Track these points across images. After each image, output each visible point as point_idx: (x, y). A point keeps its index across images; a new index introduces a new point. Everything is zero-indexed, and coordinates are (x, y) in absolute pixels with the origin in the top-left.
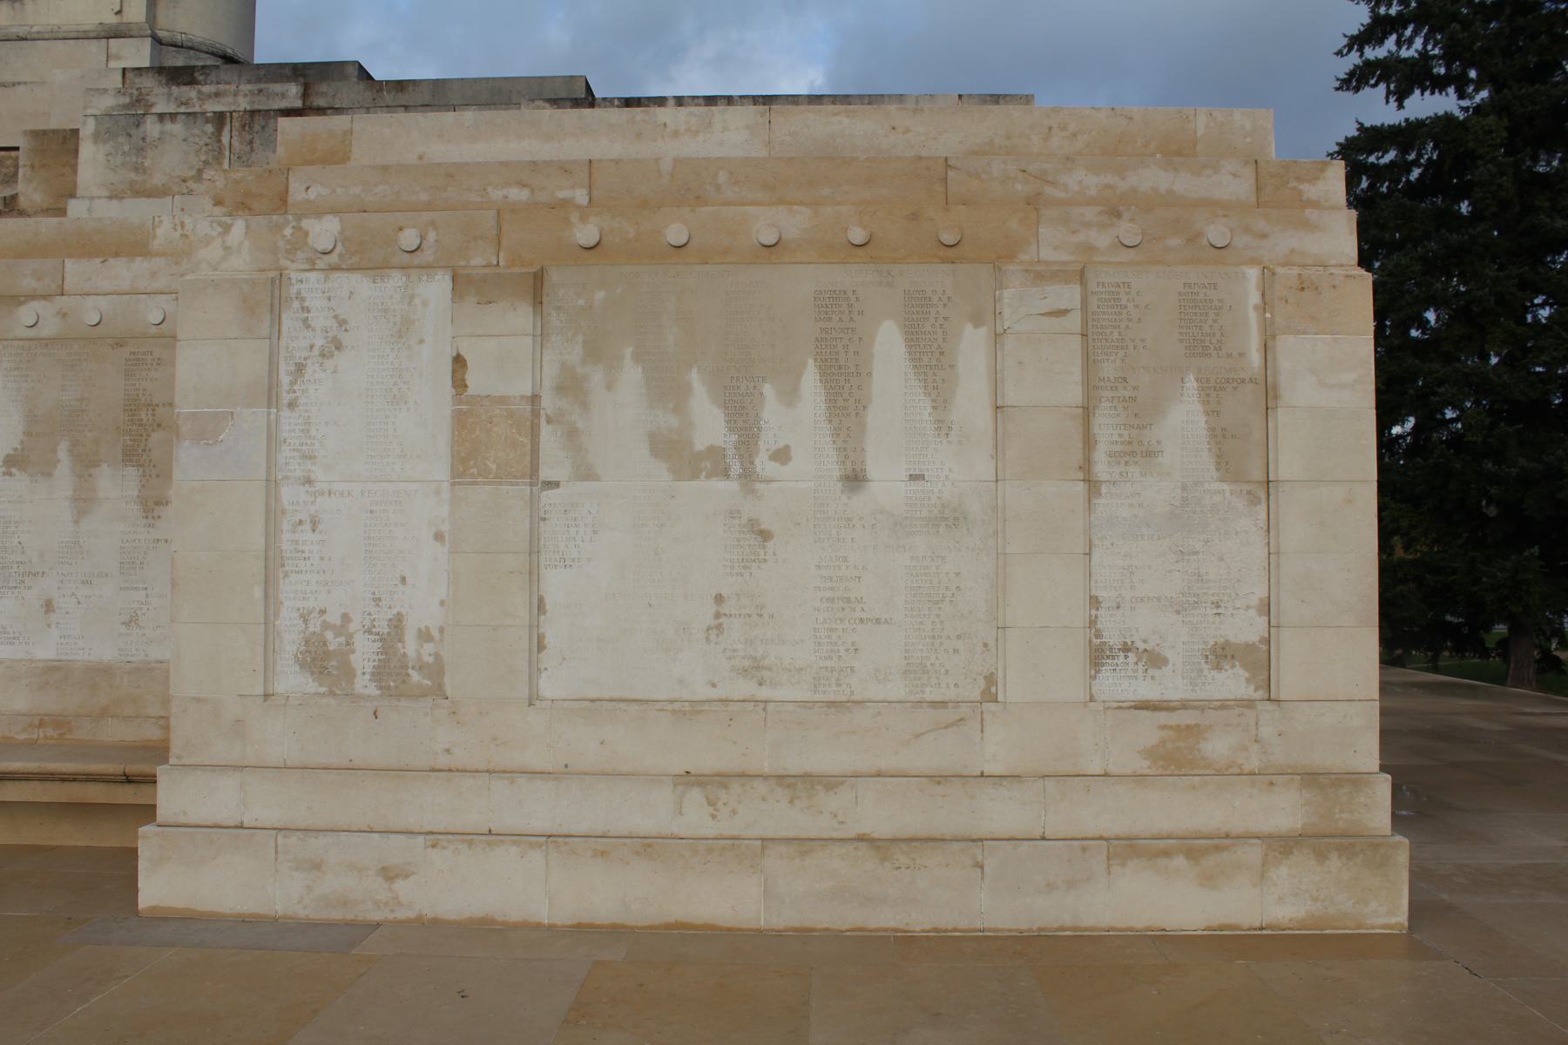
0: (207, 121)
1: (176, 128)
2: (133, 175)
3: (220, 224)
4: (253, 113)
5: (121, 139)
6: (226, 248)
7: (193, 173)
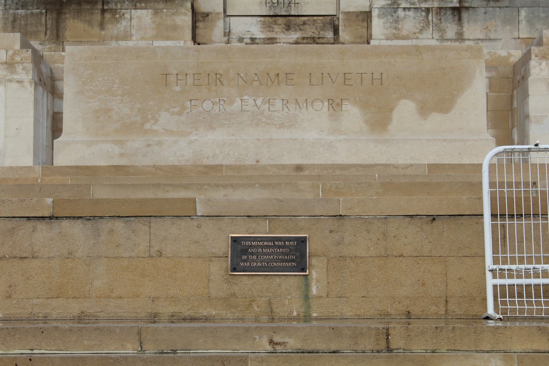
0: (422, 11)
1: (411, 13)
2: (394, 31)
3: (538, 62)
4: (440, 8)
5: (389, 17)
6: (541, 69)
7: (418, 31)
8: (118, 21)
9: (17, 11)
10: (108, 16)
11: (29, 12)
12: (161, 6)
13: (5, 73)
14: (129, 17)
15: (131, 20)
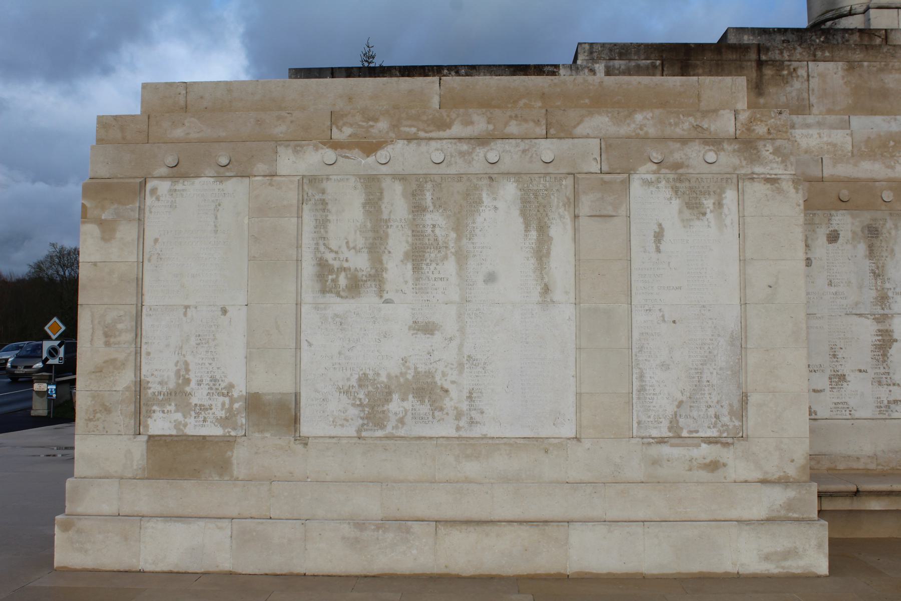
8: (786, 81)
9: (611, 63)
10: (768, 72)
11: (633, 63)
12: (858, 56)
13: (736, 161)
14: (805, 75)
15: (808, 80)
